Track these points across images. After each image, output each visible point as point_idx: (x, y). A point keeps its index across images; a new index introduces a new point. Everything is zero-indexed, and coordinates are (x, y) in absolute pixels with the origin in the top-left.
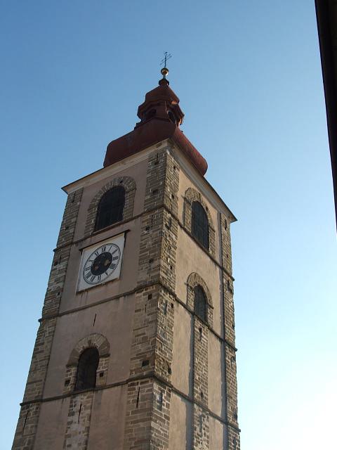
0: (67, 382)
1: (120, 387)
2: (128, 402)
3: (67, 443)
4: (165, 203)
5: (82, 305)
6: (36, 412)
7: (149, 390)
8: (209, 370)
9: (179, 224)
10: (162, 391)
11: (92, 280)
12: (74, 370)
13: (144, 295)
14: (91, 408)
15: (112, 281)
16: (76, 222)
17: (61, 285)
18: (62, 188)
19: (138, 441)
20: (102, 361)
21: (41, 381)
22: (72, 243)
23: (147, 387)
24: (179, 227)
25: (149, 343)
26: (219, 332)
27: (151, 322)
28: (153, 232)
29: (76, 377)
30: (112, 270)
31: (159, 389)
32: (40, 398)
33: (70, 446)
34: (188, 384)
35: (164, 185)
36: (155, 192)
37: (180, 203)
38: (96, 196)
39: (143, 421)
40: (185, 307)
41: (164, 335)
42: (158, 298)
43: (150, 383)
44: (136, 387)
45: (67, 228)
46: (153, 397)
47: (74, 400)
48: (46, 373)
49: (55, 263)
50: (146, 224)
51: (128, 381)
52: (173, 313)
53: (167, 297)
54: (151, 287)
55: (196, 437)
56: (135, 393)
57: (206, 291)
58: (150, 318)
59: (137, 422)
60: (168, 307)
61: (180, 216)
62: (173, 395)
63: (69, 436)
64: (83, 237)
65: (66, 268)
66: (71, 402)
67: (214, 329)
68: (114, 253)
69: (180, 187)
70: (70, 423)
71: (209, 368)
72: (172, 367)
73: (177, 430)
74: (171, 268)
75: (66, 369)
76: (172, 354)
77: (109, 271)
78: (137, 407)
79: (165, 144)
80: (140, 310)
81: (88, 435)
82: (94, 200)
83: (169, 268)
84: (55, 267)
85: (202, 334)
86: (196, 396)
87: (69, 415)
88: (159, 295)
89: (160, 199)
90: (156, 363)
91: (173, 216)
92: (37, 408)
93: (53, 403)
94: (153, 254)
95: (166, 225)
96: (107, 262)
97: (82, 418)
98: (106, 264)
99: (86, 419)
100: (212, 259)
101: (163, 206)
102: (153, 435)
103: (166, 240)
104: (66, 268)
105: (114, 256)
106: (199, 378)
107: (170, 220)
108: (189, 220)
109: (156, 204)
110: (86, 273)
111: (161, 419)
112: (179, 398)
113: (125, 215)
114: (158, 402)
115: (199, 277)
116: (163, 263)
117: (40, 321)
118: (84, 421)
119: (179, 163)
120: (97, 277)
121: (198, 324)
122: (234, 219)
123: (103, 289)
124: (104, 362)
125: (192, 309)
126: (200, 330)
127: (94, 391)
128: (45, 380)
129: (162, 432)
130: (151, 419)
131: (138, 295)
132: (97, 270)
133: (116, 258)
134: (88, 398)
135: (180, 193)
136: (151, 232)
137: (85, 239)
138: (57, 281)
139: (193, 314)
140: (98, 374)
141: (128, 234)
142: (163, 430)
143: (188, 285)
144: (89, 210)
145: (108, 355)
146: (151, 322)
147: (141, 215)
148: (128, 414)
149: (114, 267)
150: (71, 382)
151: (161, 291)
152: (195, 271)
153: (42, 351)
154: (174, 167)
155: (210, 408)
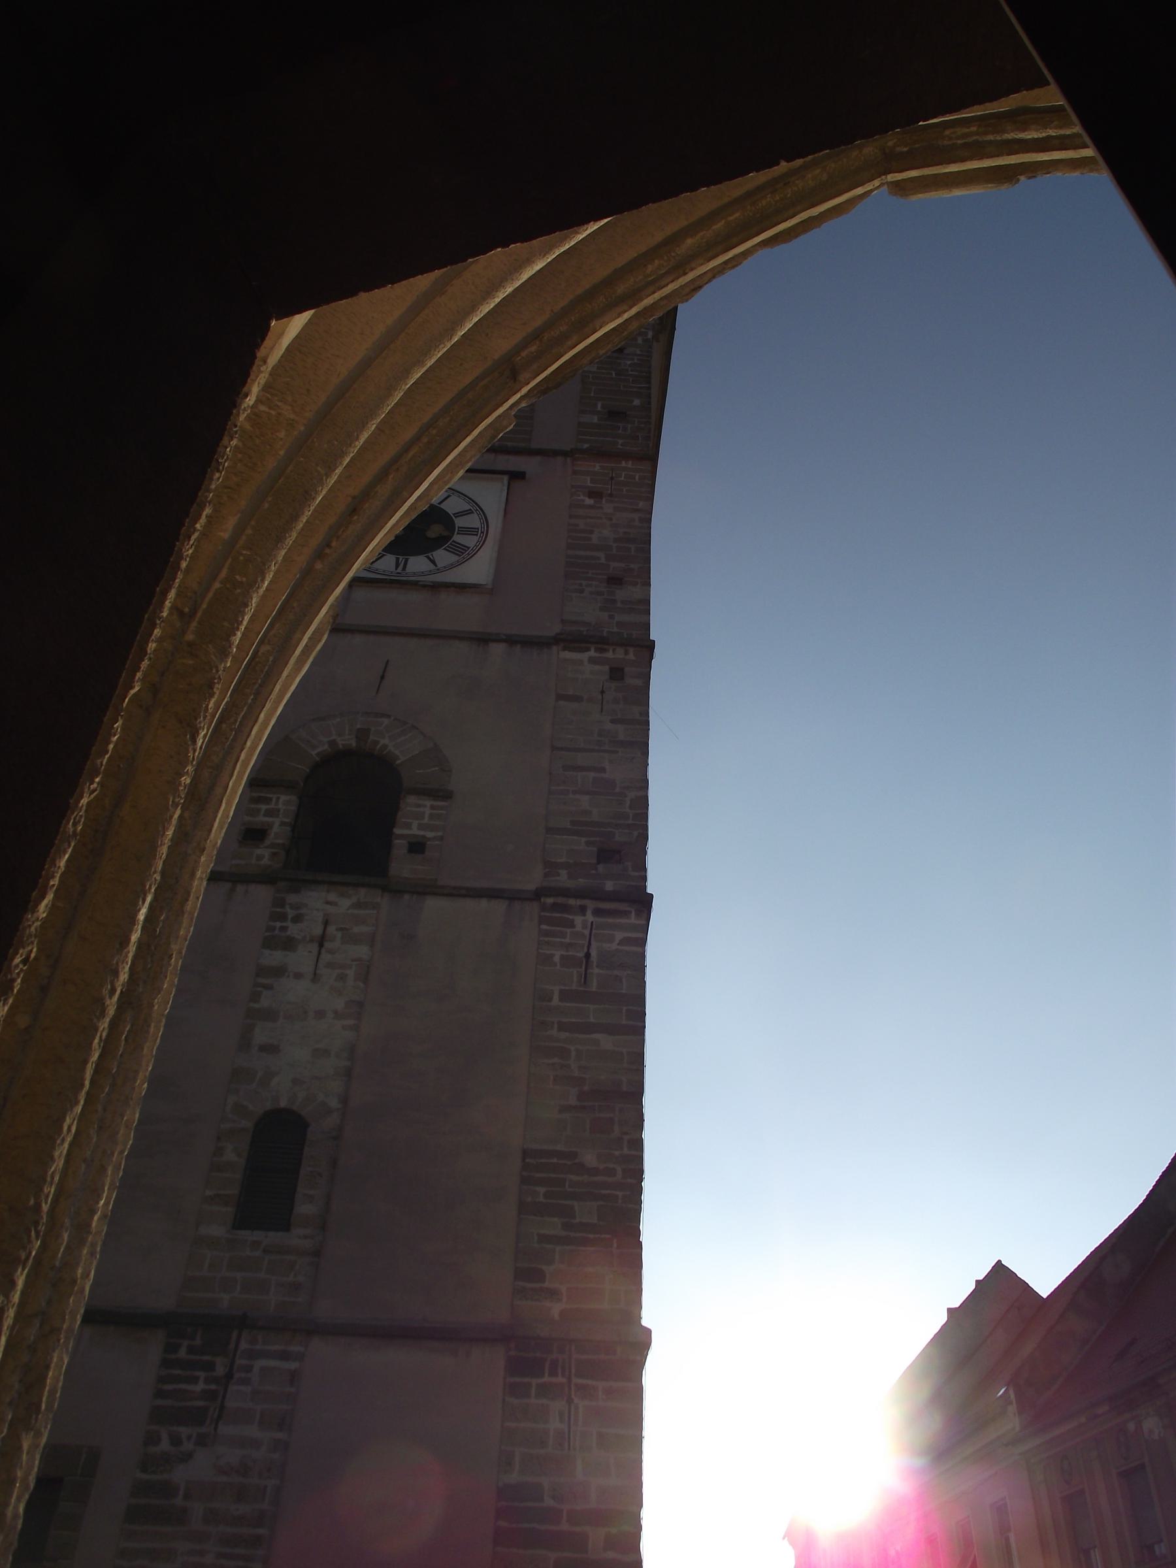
7: (626, 941)
12: (285, 803)
13: (592, 661)
15: (461, 587)
33: (271, 1049)
47: (292, 898)
51: (538, 895)
77: (442, 556)
87: (270, 943)
96: (435, 531)
99: (351, 973)
118: (342, 978)
134: (358, 905)
145: (447, 796)
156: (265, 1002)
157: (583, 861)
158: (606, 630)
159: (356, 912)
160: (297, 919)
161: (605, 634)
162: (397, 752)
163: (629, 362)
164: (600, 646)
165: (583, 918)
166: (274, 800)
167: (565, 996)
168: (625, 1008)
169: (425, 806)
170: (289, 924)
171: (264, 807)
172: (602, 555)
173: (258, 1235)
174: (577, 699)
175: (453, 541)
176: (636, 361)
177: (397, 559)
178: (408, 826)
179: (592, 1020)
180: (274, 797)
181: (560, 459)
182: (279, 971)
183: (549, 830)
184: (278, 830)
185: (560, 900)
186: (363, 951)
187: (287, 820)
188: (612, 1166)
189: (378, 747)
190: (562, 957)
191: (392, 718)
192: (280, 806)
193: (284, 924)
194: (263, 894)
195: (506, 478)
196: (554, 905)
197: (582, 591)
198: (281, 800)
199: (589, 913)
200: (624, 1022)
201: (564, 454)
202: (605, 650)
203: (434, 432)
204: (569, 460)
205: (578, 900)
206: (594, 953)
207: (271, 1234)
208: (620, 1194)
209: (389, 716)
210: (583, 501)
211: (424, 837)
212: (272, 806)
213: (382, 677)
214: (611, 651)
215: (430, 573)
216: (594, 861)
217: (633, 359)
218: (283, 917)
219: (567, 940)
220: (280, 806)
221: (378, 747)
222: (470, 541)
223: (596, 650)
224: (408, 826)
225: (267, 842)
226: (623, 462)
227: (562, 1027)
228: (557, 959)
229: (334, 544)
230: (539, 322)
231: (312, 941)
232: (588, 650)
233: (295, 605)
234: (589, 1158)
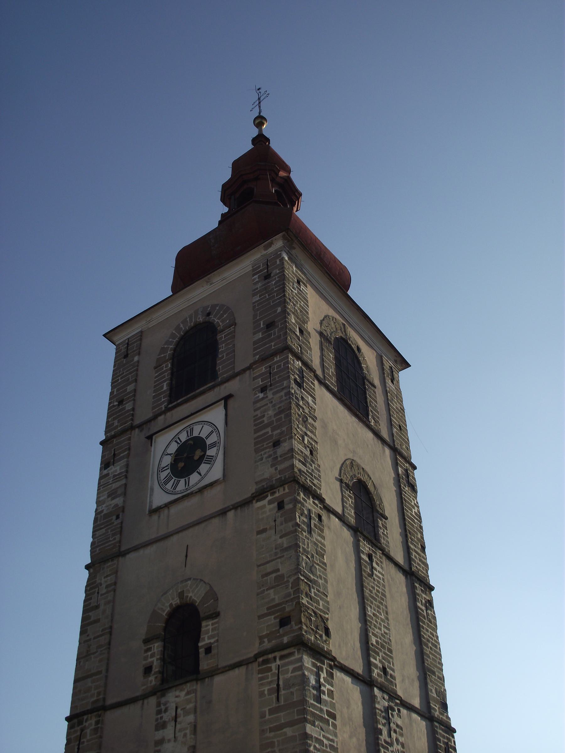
0: (148, 670)
1: (243, 669)
2: (262, 694)
4: (289, 343)
5: (162, 532)
6: (96, 730)
7: (294, 670)
8: (392, 627)
9: (316, 377)
10: (320, 669)
11: (175, 486)
12: (157, 647)
13: (270, 502)
14: (195, 712)
16: (135, 390)
17: (119, 501)
18: (104, 335)
20: (207, 626)
21: (99, 673)
22: (132, 428)
24: (316, 382)
25: (287, 587)
26: (400, 558)
27: (287, 549)
28: (274, 394)
29: (163, 660)
30: (208, 466)
31: (314, 665)
34: (359, 653)
35: (285, 313)
36: (270, 326)
37: (314, 341)
38: (167, 343)
39: (290, 724)
40: (341, 518)
41: (311, 569)
42: (295, 506)
43: (297, 656)
44: (273, 666)
45: (121, 402)
46: (304, 680)
47: (163, 700)
48: (108, 660)
49: (105, 464)
50: (260, 382)
51: (256, 657)
52: (322, 531)
53: (310, 503)
54: (281, 489)
55: (384, 747)
56: (271, 677)
57: (371, 489)
58: (285, 542)
59: (280, 727)
60: (313, 522)
61: (316, 363)
62: (338, 674)
64: (150, 415)
65: (127, 471)
66: (159, 705)
67: (392, 554)
68: (207, 438)
69: (310, 315)
70: (160, 742)
71: (391, 622)
72: (330, 625)
73: (351, 737)
74: (311, 453)
76: (328, 603)
77: (203, 468)
78: (278, 699)
79: (278, 243)
80: (264, 531)
82: (163, 350)
83: (308, 453)
84: (105, 472)
85: (375, 565)
86: (376, 672)
88: (296, 501)
89: (279, 337)
90: (303, 620)
91: (305, 364)
92: (97, 723)
93: (125, 710)
94: (279, 431)
95: (295, 380)
96: (198, 453)
97: (180, 730)
98: (196, 458)
99: (188, 731)
100: (377, 434)
101: (288, 349)
102: (312, 748)
103: (298, 405)
104: (127, 471)
105: (209, 442)
106: (377, 642)
107: (301, 371)
108: (332, 370)
109: (273, 346)
110: (163, 475)
111: (321, 719)
112: (348, 679)
113: (222, 369)
114: (314, 688)
115: (358, 466)
116: (297, 446)
117: (87, 567)
118: (185, 735)
119: (305, 275)
120: (182, 481)
121: (366, 547)
122: (405, 364)
123: (195, 500)
124: (210, 627)
125: (352, 521)
126: (370, 556)
127: (197, 680)
128: (107, 670)
129: (325, 741)
130: (305, 720)
131: (260, 504)
132: (182, 468)
133: (213, 445)
134: (188, 693)
135: (312, 326)
136: (270, 394)
137: (155, 417)
138: (112, 495)
139: (355, 530)
140: (202, 651)
141: (231, 402)
142: (328, 739)
143: (341, 481)
144: (155, 368)
145: (216, 615)
146: (287, 549)
147: (249, 368)
148: (263, 715)
149: (211, 460)
150: (155, 669)
151: (299, 494)
152: (350, 456)
153: (97, 621)
154: (298, 282)
155: (400, 693)
157: (274, 630)
158: (274, 479)
160: (166, 710)
162: (195, 599)
163: (273, 282)
164: (272, 491)
166: (153, 648)
168: (296, 710)
170: (163, 714)
171: (149, 653)
172: (269, 430)
175: (207, 456)
176: (277, 279)
179: (283, 721)
180: (152, 646)
185: (265, 657)
189: (188, 599)
191: (192, 579)
196: (263, 661)
197: (262, 459)
200: (296, 717)
202: (275, 493)
205: (273, 654)
206: (281, 683)
209: (190, 579)
210: (259, 396)
211: (210, 643)
213: (186, 556)
215: (200, 481)
216: (278, 628)
219: (270, 680)
220: (156, 650)
221: (188, 599)
225: (153, 672)
227: (271, 730)
228: (266, 692)
232: (267, 496)
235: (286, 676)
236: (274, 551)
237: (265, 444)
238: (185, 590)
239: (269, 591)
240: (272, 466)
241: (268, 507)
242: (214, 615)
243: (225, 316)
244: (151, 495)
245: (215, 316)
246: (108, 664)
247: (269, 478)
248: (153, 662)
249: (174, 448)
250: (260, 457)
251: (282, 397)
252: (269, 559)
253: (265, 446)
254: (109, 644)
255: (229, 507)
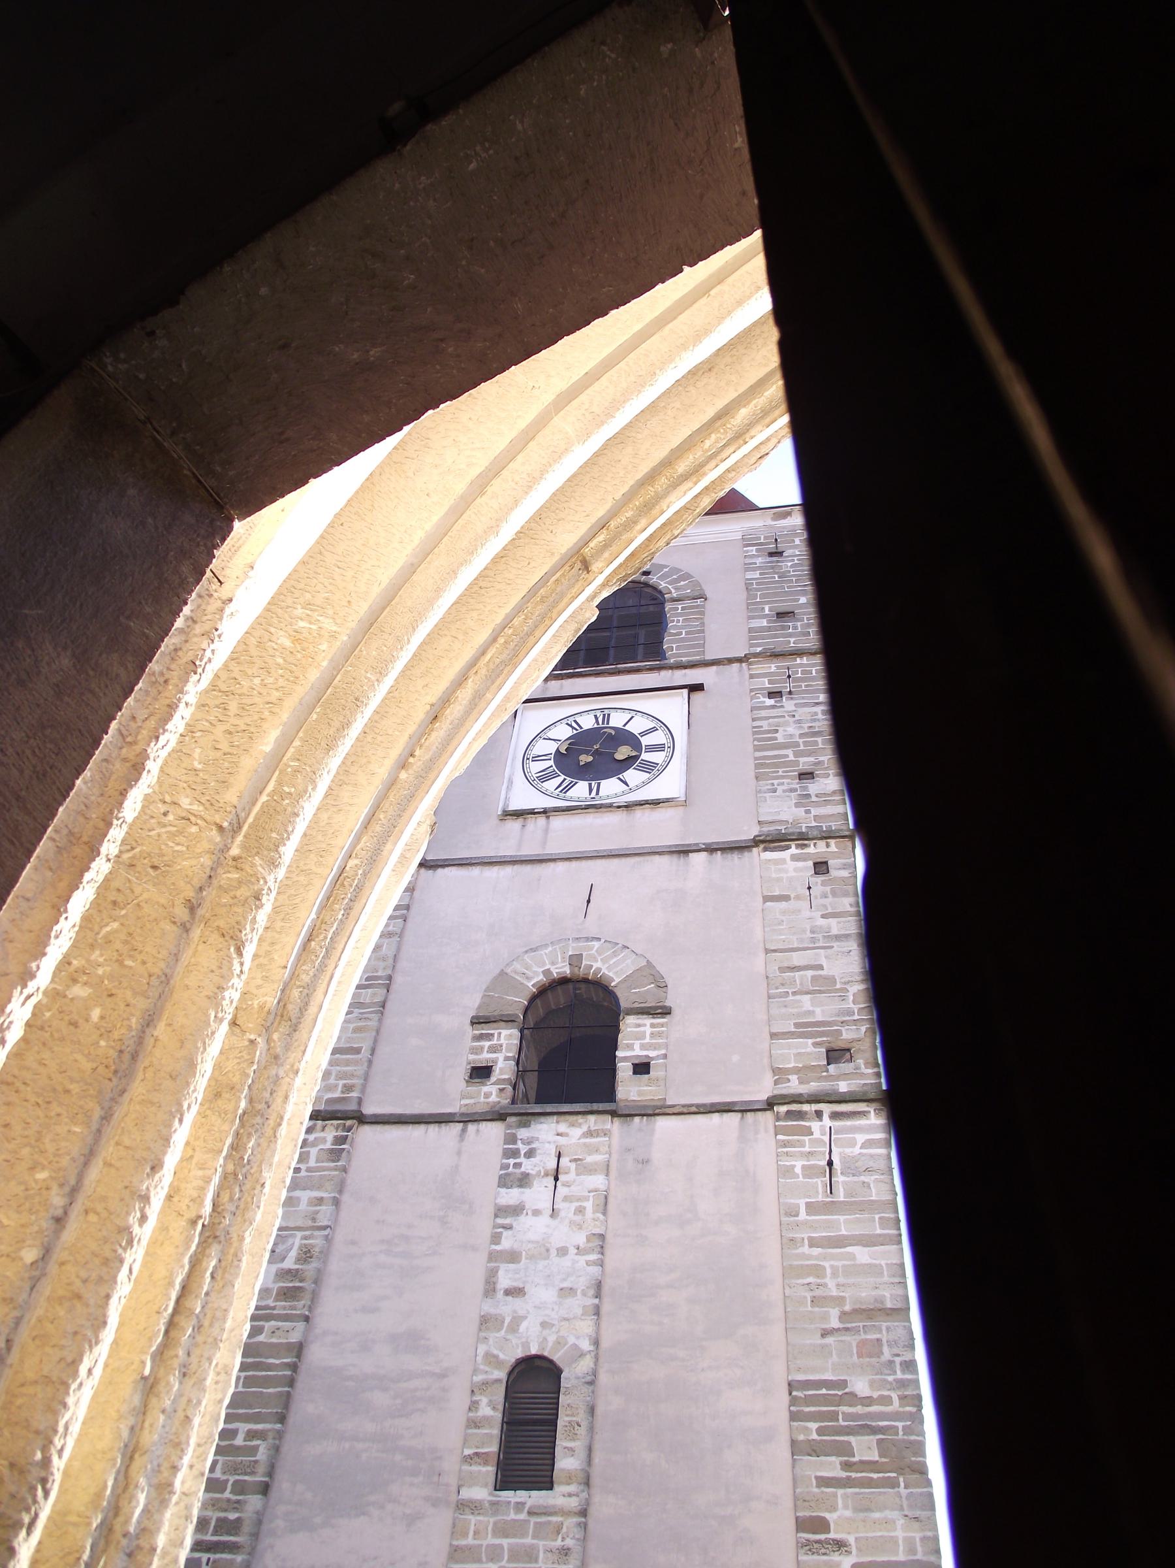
2: (787, 1172)
3: (505, 1280)
5: (528, 851)
12: (508, 1038)
13: (794, 858)
15: (656, 803)
19: (855, 1311)
23: (860, 1129)
25: (843, 999)
32: (353, 1107)
33: (515, 1292)
47: (523, 1133)
48: (378, 1032)
51: (770, 1104)
59: (840, 1242)
63: (513, 1257)
66: (511, 1139)
75: (470, 1032)
77: (633, 775)
81: (601, 1263)
87: (505, 1181)
96: (623, 753)
97: (566, 1199)
99: (589, 1205)
118: (580, 1211)
128: (373, 1051)
132: (587, 764)
134: (590, 1133)
145: (666, 1012)
146: (838, 938)
156: (506, 1243)
159: (588, 1140)
160: (530, 1154)
161: (804, 830)
162: (611, 974)
163: (789, 564)
165: (820, 1123)
167: (811, 1208)
168: (877, 1217)
169: (645, 1025)
170: (522, 1159)
171: (487, 1044)
172: (790, 752)
173: (521, 1495)
174: (786, 898)
177: (590, 785)
178: (630, 1047)
179: (844, 1232)
180: (496, 1032)
181: (736, 666)
182: (517, 1210)
183: (773, 1036)
184: (504, 1068)
185: (794, 1107)
186: (598, 1181)
187: (511, 1055)
188: (886, 1393)
190: (803, 1167)
191: (603, 941)
192: (502, 1041)
193: (518, 1161)
194: (494, 1132)
195: (685, 691)
197: (775, 791)
198: (502, 1036)
199: (826, 1117)
200: (879, 1231)
201: (739, 660)
202: (806, 846)
203: (511, 631)
204: (744, 664)
207: (534, 1493)
208: (900, 1424)
209: (599, 939)
210: (764, 702)
211: (647, 1056)
212: (495, 1042)
213: (589, 901)
214: (812, 846)
215: (624, 793)
217: (793, 560)
218: (515, 1153)
219: (807, 1149)
220: (502, 1041)
222: (658, 757)
223: (798, 846)
224: (630, 1047)
225: (493, 1079)
226: (798, 659)
227: (813, 1243)
228: (798, 1170)
229: (417, 753)
230: (601, 512)
231: (546, 1175)
232: (789, 847)
233: (382, 816)
234: (861, 1386)
235: (848, 1151)
236: (809, 935)
237: (780, 770)
238: (584, 954)
239: (798, 997)
240: (797, 805)
241: (792, 865)
242: (660, 1011)
243: (682, 583)
244: (509, 789)
245: (662, 578)
246: (375, 1041)
247: (791, 821)
248: (495, 1061)
249: (564, 733)
250: (769, 787)
251: (816, 714)
252: (795, 946)
253: (780, 773)
254: (383, 1005)
255: (697, 844)
